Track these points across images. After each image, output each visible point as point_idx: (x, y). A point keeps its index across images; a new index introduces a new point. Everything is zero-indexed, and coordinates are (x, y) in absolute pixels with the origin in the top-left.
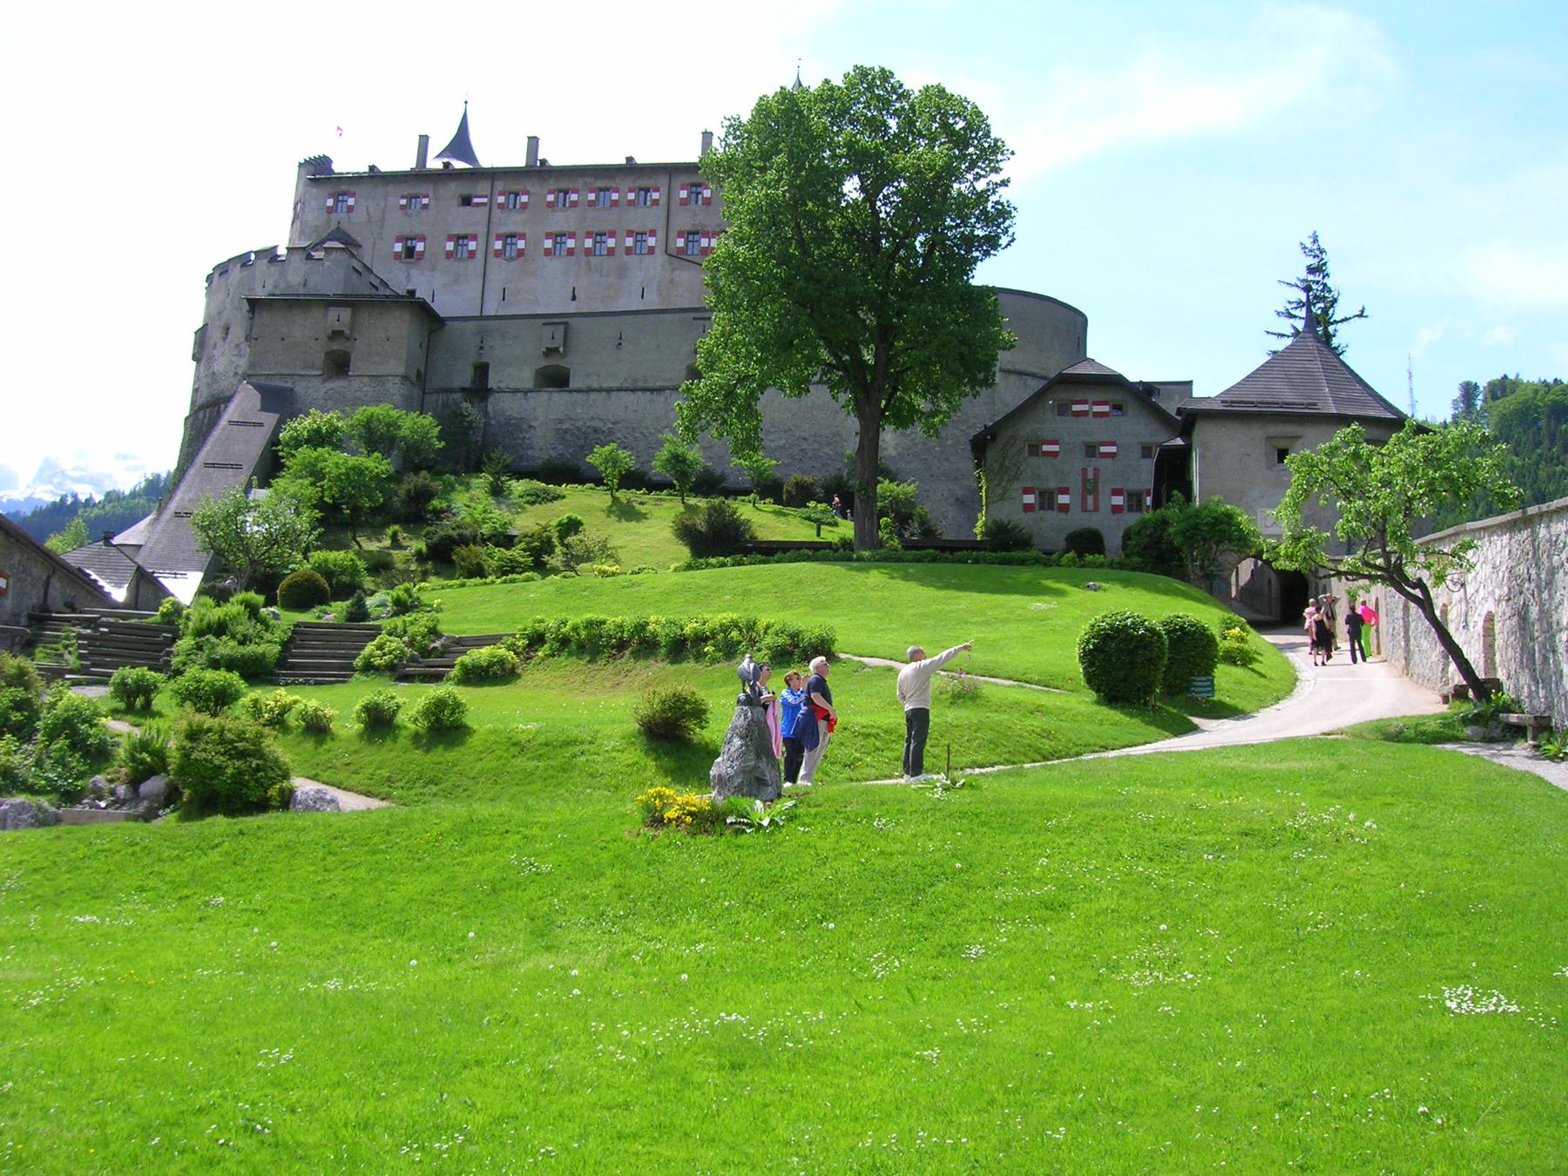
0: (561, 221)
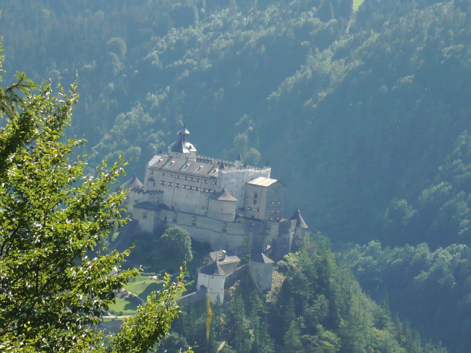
0: (185, 183)
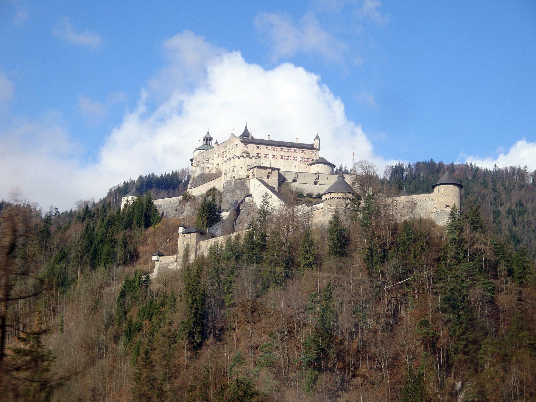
0: (282, 154)
